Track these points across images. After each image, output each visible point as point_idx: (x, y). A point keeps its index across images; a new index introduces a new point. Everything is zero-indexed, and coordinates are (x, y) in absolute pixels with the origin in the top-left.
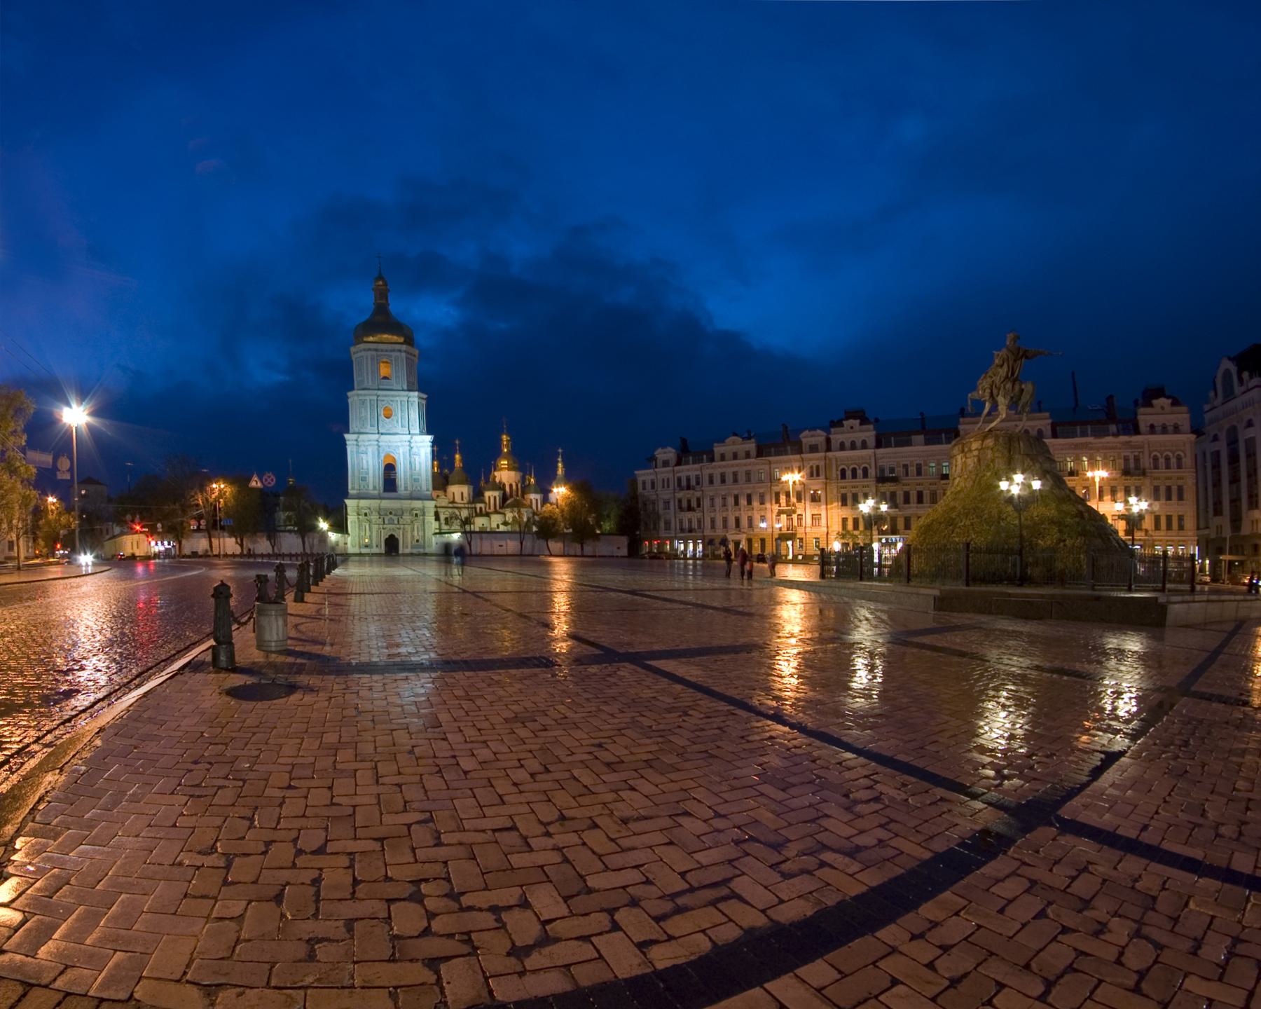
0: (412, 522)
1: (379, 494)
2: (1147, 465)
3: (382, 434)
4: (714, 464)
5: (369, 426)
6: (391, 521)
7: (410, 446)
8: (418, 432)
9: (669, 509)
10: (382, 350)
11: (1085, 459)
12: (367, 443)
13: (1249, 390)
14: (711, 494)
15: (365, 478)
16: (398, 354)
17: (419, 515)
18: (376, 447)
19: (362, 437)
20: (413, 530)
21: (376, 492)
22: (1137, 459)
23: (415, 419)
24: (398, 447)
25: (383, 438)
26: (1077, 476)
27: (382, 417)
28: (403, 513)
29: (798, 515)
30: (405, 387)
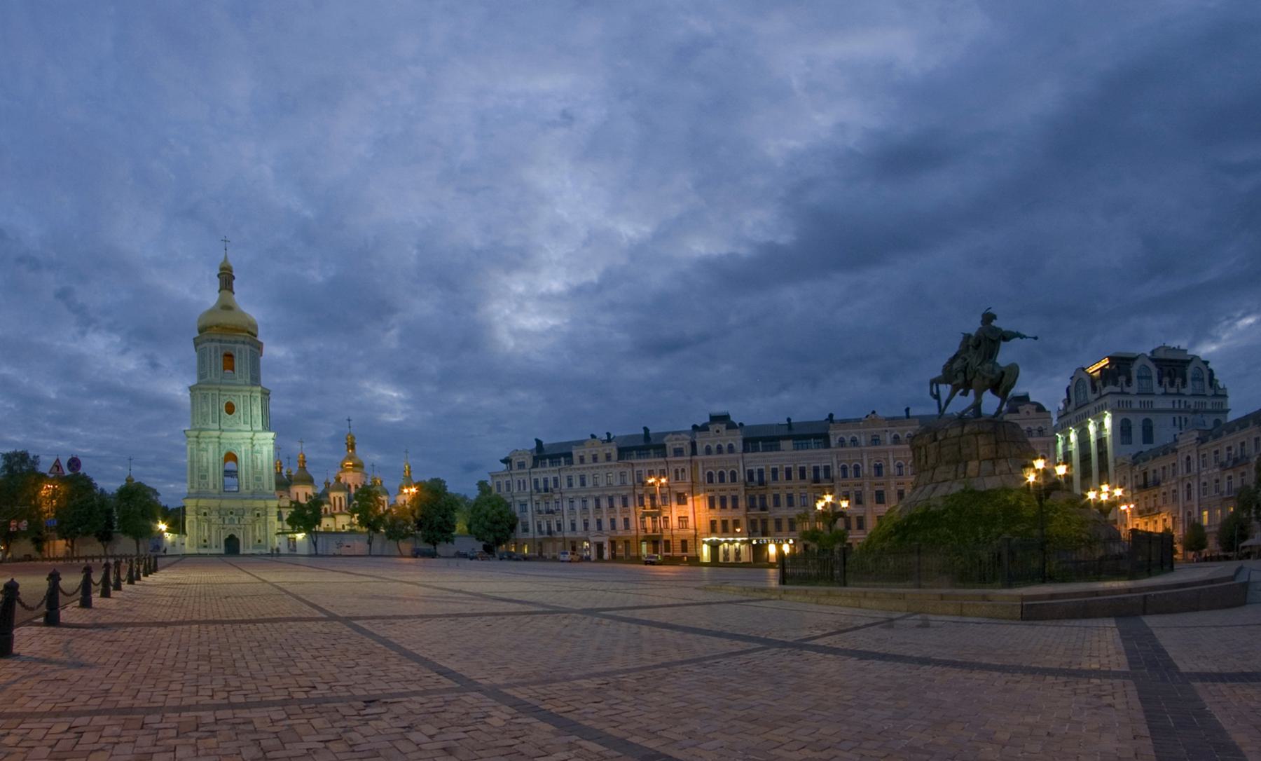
0: (253, 522)
3: (223, 431)
5: (210, 423)
6: (232, 521)
7: (252, 443)
8: (260, 428)
9: (526, 511)
12: (207, 440)
13: (1101, 397)
14: (571, 496)
17: (260, 515)
18: (217, 444)
19: (203, 434)
20: (254, 530)
23: (258, 415)
24: (239, 444)
25: (225, 434)
27: (224, 413)
28: (244, 513)
29: (664, 518)
30: (248, 381)
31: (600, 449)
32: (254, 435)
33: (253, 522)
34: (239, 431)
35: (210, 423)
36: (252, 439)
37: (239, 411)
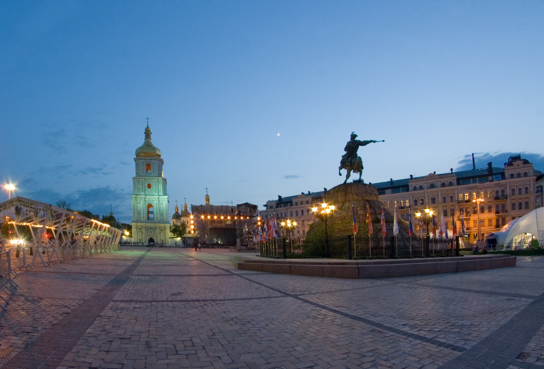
0: (160, 232)
1: (146, 221)
2: (508, 193)
3: (146, 195)
4: (292, 207)
5: (141, 192)
6: (151, 232)
7: (158, 200)
8: (162, 194)
10: (147, 160)
11: (474, 194)
15: (140, 213)
16: (154, 161)
17: (163, 230)
18: (144, 201)
19: (138, 196)
20: (160, 236)
21: (144, 220)
22: (503, 191)
23: (161, 189)
24: (153, 201)
25: (147, 197)
26: (470, 202)
27: (147, 188)
28: (156, 229)
30: (157, 175)
31: (304, 199)
32: (159, 197)
33: (160, 232)
34: (153, 195)
35: (141, 192)
36: (158, 198)
37: (153, 187)
